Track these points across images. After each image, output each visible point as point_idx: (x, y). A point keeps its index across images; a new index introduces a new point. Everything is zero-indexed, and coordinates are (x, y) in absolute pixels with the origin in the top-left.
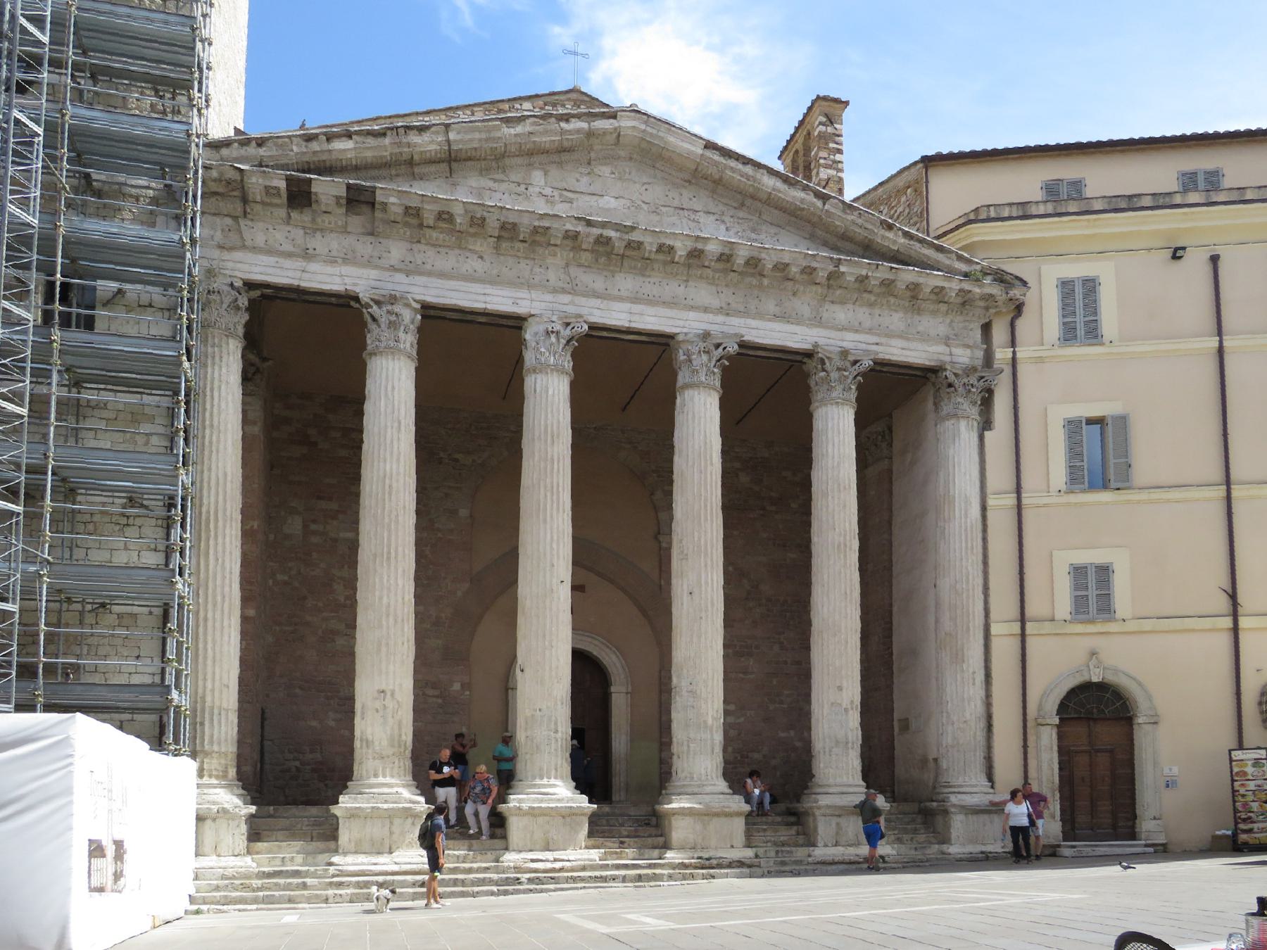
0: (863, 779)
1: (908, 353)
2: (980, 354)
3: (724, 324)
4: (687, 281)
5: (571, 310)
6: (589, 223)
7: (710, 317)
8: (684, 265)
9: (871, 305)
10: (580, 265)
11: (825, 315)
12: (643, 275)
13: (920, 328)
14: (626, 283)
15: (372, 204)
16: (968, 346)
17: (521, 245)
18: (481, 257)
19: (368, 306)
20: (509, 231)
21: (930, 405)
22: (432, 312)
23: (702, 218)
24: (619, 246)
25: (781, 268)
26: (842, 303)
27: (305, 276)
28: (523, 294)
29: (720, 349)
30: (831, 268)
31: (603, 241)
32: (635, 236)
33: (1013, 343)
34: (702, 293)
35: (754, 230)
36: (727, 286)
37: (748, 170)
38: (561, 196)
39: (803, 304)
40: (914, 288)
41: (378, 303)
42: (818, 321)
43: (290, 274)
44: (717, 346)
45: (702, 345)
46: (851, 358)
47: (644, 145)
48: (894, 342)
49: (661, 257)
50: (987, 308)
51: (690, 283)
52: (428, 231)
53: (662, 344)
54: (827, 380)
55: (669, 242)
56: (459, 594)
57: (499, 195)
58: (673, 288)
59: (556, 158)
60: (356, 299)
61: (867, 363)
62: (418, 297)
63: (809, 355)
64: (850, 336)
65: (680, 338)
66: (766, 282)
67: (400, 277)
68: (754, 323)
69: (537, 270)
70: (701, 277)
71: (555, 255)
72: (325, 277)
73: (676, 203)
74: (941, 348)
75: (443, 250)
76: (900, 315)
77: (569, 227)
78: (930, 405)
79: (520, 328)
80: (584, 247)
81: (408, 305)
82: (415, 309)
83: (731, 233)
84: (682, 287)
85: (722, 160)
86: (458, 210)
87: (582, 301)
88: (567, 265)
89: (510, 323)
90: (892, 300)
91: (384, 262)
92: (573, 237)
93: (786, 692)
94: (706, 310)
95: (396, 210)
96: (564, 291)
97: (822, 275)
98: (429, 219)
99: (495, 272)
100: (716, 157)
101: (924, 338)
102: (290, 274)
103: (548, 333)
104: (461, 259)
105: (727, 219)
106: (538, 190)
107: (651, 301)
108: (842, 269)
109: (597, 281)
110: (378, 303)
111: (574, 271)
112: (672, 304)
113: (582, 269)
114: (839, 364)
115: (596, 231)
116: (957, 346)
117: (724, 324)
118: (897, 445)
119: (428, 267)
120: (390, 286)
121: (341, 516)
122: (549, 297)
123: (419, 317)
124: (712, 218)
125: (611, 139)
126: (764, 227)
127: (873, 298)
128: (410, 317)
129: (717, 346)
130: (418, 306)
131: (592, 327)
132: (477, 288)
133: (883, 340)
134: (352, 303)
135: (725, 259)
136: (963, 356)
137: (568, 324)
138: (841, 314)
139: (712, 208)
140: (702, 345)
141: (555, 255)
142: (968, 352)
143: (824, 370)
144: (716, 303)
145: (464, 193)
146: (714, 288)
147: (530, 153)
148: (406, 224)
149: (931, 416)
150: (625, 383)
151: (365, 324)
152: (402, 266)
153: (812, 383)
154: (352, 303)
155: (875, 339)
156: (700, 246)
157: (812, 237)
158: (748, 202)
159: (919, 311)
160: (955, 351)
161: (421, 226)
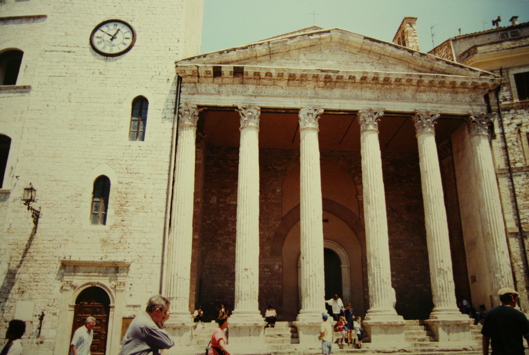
0: (458, 306)
1: (453, 110)
2: (485, 108)
3: (377, 104)
4: (361, 89)
5: (317, 104)
7: (371, 102)
8: (360, 83)
9: (436, 92)
10: (319, 87)
11: (418, 97)
12: (344, 88)
13: (458, 99)
14: (337, 92)
15: (242, 73)
17: (297, 82)
18: (282, 88)
19: (241, 110)
20: (292, 77)
21: (467, 131)
22: (264, 110)
23: (365, 65)
24: (334, 78)
25: (398, 80)
27: (218, 101)
28: (298, 100)
29: (377, 115)
30: (419, 78)
32: (340, 74)
34: (368, 94)
35: (386, 67)
36: (377, 89)
37: (381, 45)
38: (311, 62)
40: (453, 83)
41: (245, 109)
43: (214, 101)
44: (375, 113)
45: (369, 114)
46: (431, 114)
47: (341, 41)
48: (447, 106)
49: (350, 81)
50: (485, 89)
51: (363, 90)
52: (263, 81)
53: (354, 114)
54: (422, 123)
55: (353, 75)
56: (277, 225)
57: (288, 65)
60: (237, 108)
61: (438, 116)
62: (260, 105)
63: (413, 114)
64: (429, 105)
65: (360, 111)
66: (393, 86)
67: (253, 98)
69: (303, 90)
70: (367, 87)
71: (310, 84)
72: (225, 101)
73: (355, 60)
74: (468, 107)
75: (268, 87)
76: (449, 94)
77: (314, 73)
78: (467, 131)
79: (298, 113)
80: (320, 80)
81: (255, 108)
82: (258, 110)
83: (377, 69)
84: (360, 91)
85: (371, 42)
87: (322, 100)
88: (315, 88)
89: (294, 111)
90: (445, 89)
91: (246, 94)
92: (316, 77)
93: (418, 265)
94: (370, 100)
95: (251, 73)
96: (314, 98)
97: (414, 82)
98: (263, 75)
99: (287, 93)
100: (368, 41)
101: (460, 103)
102: (214, 101)
103: (308, 114)
104: (275, 89)
105: (375, 64)
106: (302, 61)
107: (348, 98)
109: (327, 93)
110: (245, 109)
111: (317, 89)
112: (357, 98)
113: (320, 89)
114: (426, 117)
116: (474, 105)
117: (377, 104)
118: (454, 150)
119: (263, 93)
120: (249, 102)
121: (232, 195)
122: (308, 100)
123: (260, 112)
124: (369, 64)
125: (329, 40)
126: (390, 66)
127: (437, 89)
128: (256, 113)
129: (375, 113)
130: (259, 108)
131: (326, 110)
132: (281, 99)
133: (443, 105)
134: (236, 110)
135: (376, 79)
137: (316, 110)
138: (424, 96)
139: (369, 60)
140: (369, 114)
141: (310, 84)
142: (479, 107)
143: (420, 120)
146: (372, 90)
147: (299, 49)
148: (255, 79)
149: (468, 136)
150: (340, 133)
151: (240, 117)
152: (253, 94)
153: (416, 126)
154: (236, 110)
155: (440, 105)
156: (365, 75)
157: (409, 68)
158: (382, 57)
159: (457, 93)
160: (474, 107)
161: (260, 78)
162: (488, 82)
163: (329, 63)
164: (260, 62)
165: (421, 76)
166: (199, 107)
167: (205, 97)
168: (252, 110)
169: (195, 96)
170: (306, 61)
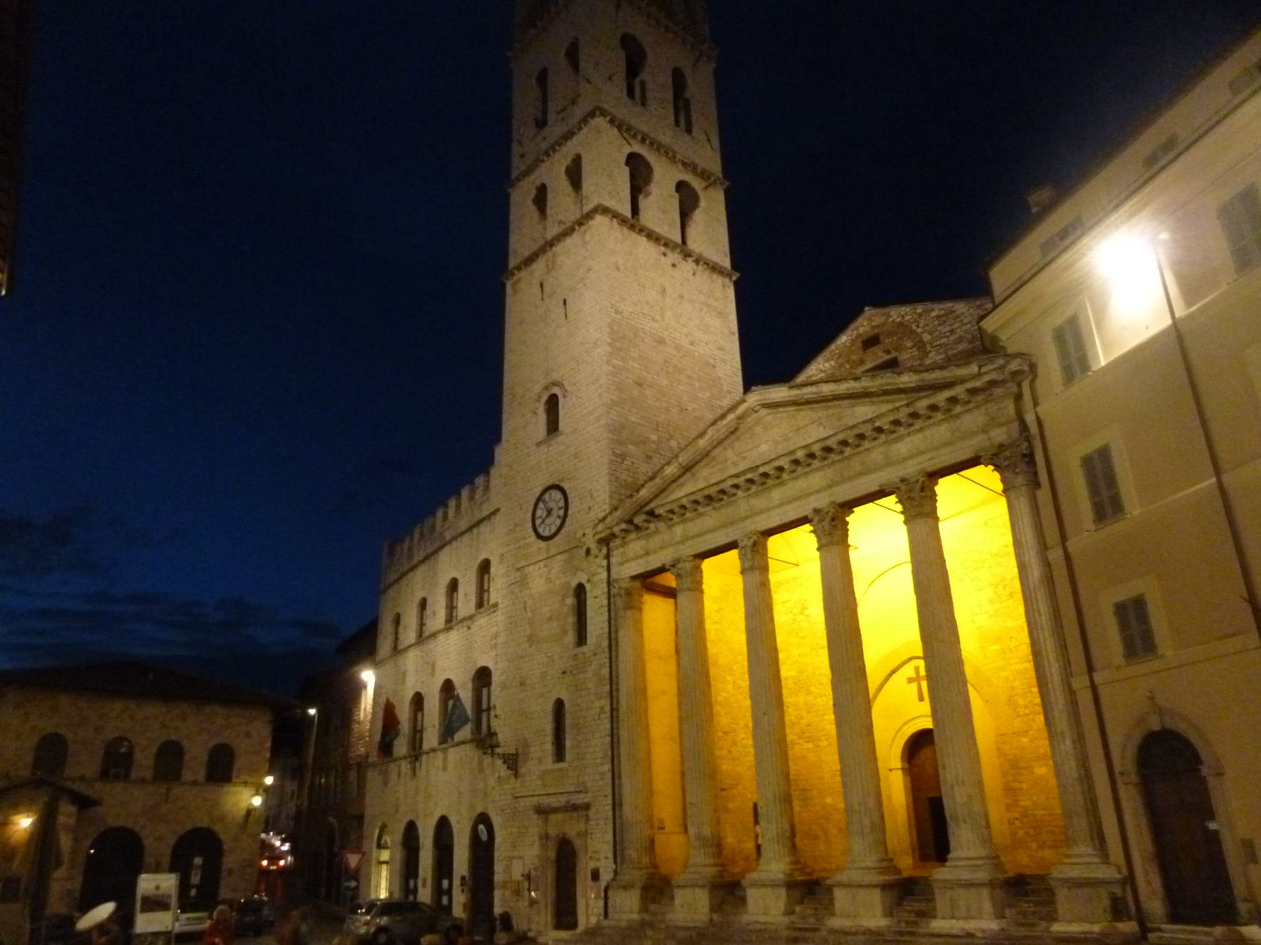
2: (1015, 426)
6: (737, 476)
7: (823, 494)
14: (777, 494)
16: (1003, 425)
26: (901, 438)
31: (751, 481)
32: (762, 470)
33: (1036, 404)
34: (816, 479)
39: (877, 455)
42: (888, 463)
48: (943, 451)
58: (802, 484)
59: (733, 437)
67: (681, 546)
68: (847, 486)
72: (654, 562)
74: (982, 437)
86: (684, 501)
94: (818, 491)
108: (877, 424)
115: (742, 479)
132: (709, 536)
136: (999, 436)
138: (902, 448)
142: (1004, 428)
144: (825, 483)
145: (681, 493)
156: (793, 457)
157: (873, 403)
159: (958, 416)
162: (994, 376)
163: (764, 447)
164: (682, 485)
165: (871, 421)
166: (634, 578)
167: (634, 563)
168: (679, 566)
169: (626, 565)
170: (735, 459)
